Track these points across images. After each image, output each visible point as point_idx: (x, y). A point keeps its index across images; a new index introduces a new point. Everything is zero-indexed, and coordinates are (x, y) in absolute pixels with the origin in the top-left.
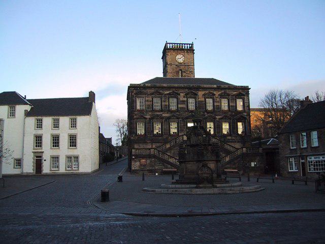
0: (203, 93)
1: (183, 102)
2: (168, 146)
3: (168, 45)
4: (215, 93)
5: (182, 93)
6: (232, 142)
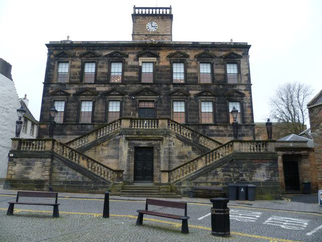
0: (168, 53)
1: (133, 68)
2: (91, 139)
3: (137, 10)
4: (189, 53)
5: (133, 53)
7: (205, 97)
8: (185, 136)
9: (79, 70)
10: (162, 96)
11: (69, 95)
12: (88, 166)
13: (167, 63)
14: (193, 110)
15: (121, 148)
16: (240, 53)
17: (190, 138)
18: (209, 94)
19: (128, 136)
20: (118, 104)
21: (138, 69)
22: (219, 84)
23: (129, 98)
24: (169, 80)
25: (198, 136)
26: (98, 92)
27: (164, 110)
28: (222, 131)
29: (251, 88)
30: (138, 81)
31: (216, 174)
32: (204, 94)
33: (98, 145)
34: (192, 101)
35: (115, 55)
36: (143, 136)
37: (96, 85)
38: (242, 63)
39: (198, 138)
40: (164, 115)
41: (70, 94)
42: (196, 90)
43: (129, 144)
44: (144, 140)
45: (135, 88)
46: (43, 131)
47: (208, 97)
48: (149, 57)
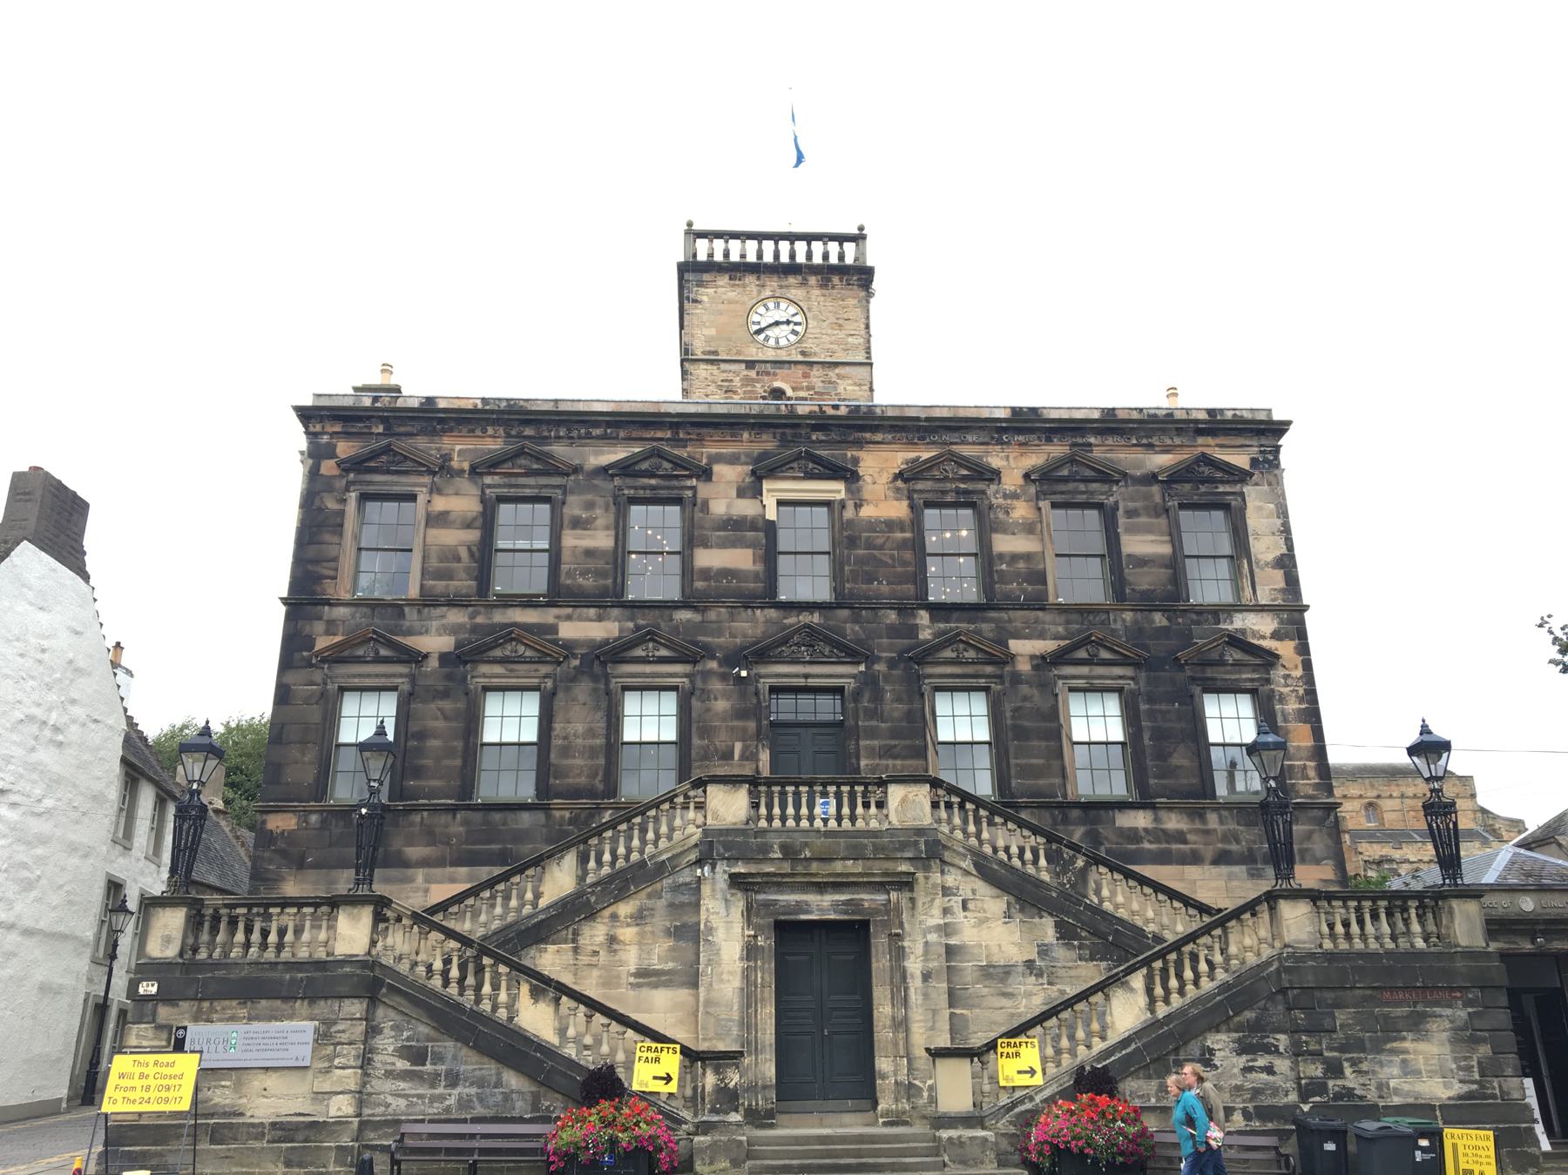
0: (898, 457)
1: (736, 529)
2: (560, 880)
3: (702, 247)
4: (995, 461)
5: (733, 460)
6: (1163, 858)
7: (1084, 670)
8: (1016, 862)
9: (473, 535)
10: (880, 667)
11: (418, 658)
12: (562, 1032)
13: (898, 509)
14: (1028, 732)
15: (710, 930)
16: (1241, 460)
17: (1045, 876)
18: (1105, 655)
19: (740, 868)
20: (670, 703)
21: (761, 534)
22: (1148, 602)
23: (724, 677)
24: (912, 587)
25: (1080, 863)
26: (569, 647)
27: (895, 733)
28: (1180, 837)
29: (1303, 622)
30: (763, 592)
31: (1206, 1059)
32: (1082, 654)
33: (592, 915)
34: (1025, 689)
35: (645, 466)
36: (815, 867)
37: (555, 611)
38: (1252, 504)
39: (1083, 874)
40: (895, 757)
41: (426, 656)
42: (1042, 636)
43: (749, 912)
44: (821, 888)
45: (752, 625)
46: (281, 844)
47: (1100, 670)
48: (810, 476)
